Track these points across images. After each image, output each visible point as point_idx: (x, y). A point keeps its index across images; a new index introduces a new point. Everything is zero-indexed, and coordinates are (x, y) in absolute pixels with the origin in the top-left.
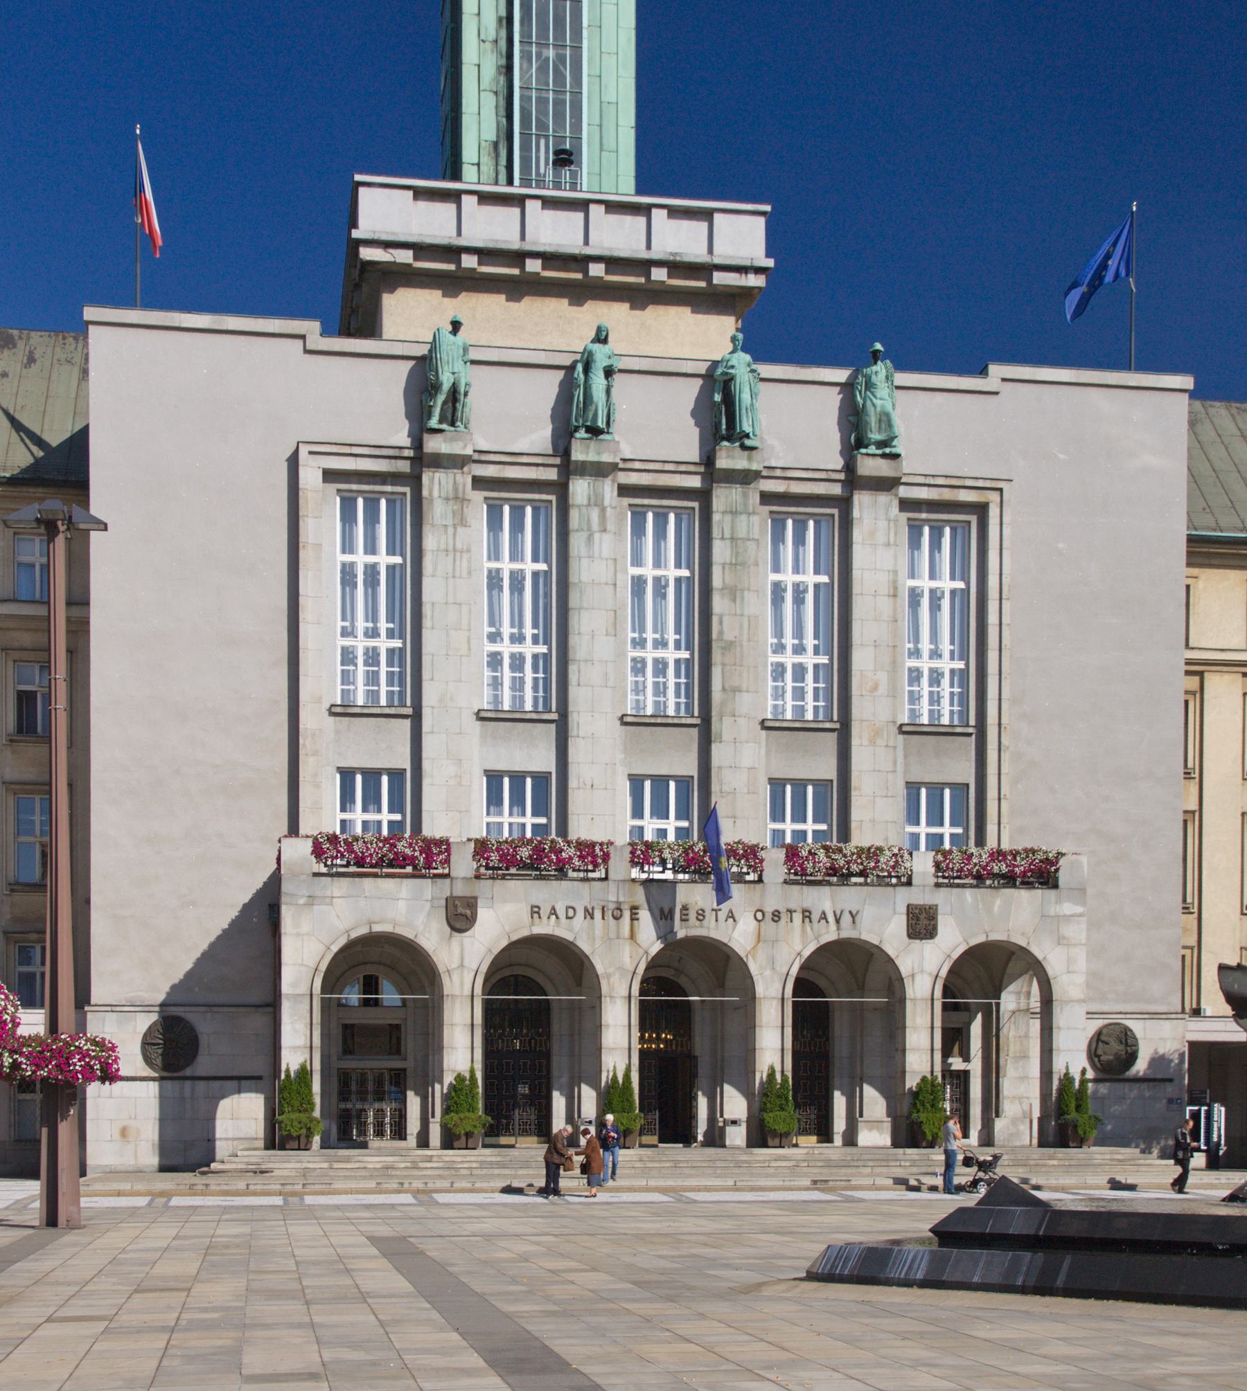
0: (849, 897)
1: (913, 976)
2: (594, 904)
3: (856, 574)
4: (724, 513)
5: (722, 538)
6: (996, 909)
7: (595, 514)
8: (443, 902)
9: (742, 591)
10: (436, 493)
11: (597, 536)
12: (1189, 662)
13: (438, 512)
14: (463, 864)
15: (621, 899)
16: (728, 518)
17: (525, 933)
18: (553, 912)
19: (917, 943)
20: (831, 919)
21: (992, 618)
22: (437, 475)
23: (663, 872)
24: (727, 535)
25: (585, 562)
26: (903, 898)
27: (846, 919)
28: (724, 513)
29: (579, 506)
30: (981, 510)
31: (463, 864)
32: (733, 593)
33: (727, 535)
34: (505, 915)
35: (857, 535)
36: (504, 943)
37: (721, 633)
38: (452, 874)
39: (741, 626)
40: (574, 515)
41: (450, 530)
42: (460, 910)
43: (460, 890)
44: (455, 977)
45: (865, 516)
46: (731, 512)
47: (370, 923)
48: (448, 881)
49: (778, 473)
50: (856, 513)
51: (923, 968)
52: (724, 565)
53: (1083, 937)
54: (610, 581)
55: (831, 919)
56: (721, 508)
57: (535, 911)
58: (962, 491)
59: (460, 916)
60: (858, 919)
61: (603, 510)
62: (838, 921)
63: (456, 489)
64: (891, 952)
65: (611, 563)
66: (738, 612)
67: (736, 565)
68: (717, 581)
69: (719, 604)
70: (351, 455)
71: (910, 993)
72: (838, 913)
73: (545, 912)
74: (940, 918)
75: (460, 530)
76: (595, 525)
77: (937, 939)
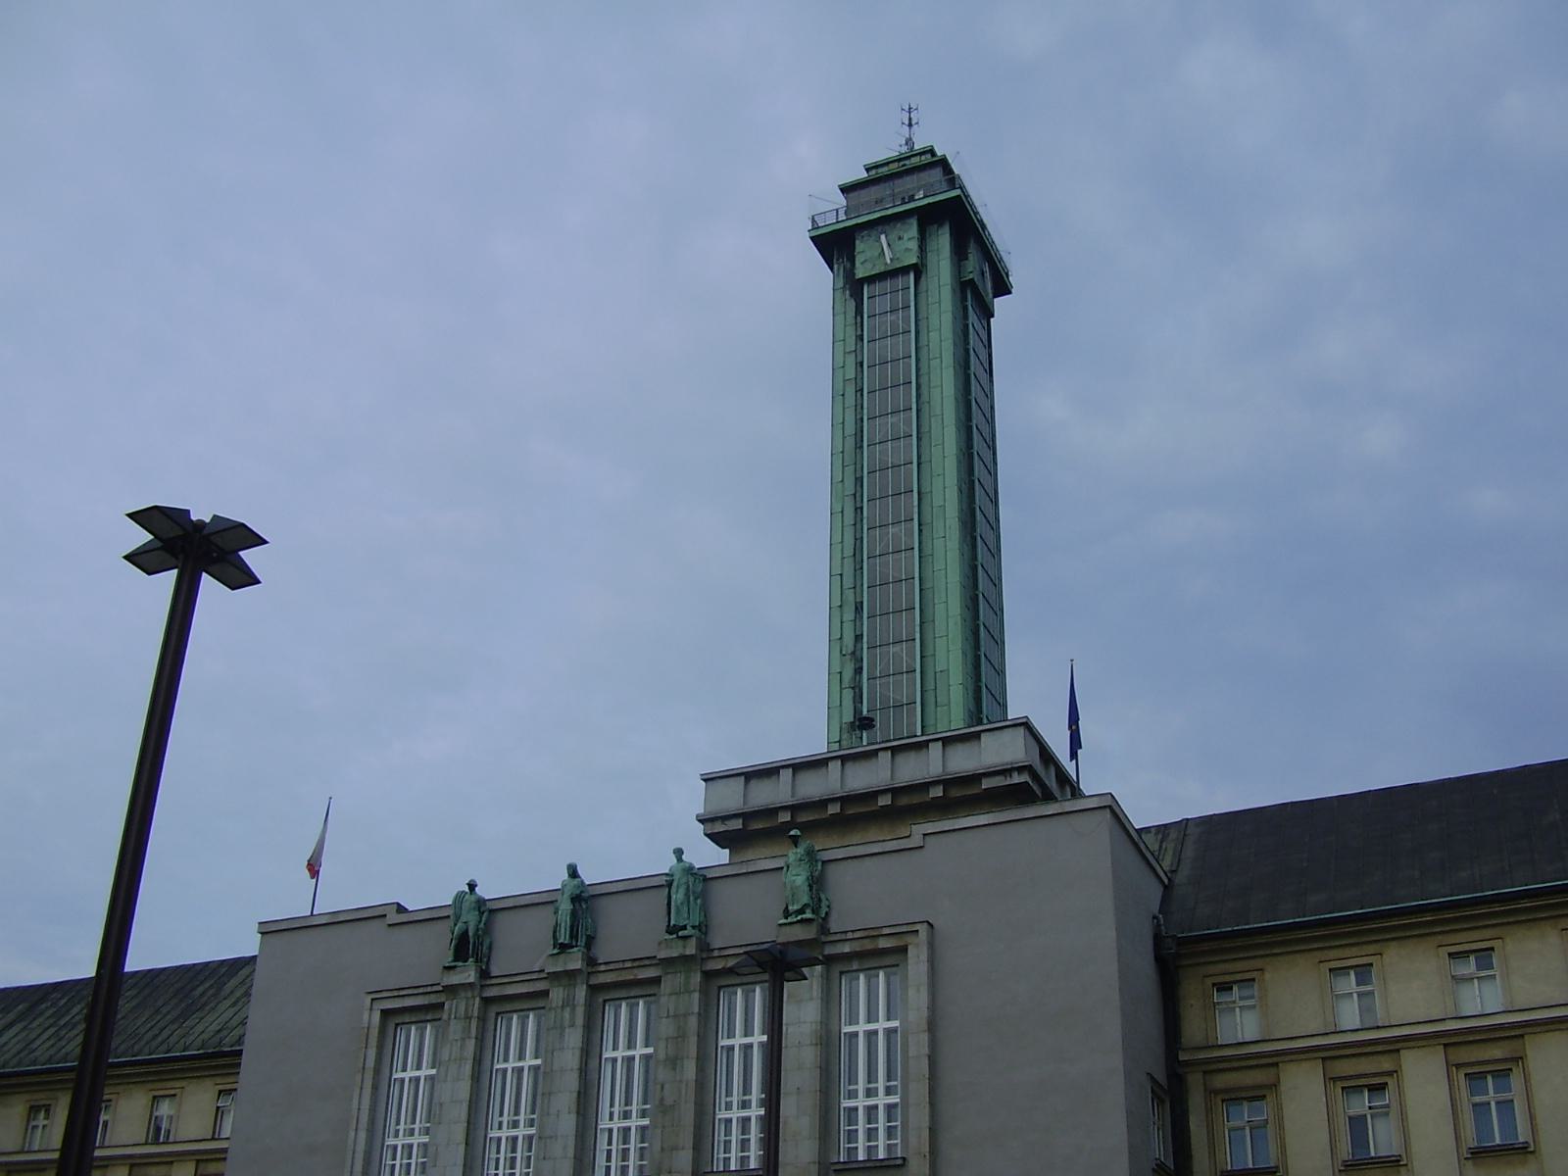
5: (668, 1017)
7: (567, 1015)
9: (682, 1059)
11: (567, 1030)
24: (671, 1013)
28: (671, 994)
30: (904, 950)
32: (674, 1062)
37: (662, 1099)
46: (676, 994)
52: (667, 1039)
56: (668, 991)
58: (881, 938)
66: (678, 1078)
75: (467, 1041)
76: (567, 1023)
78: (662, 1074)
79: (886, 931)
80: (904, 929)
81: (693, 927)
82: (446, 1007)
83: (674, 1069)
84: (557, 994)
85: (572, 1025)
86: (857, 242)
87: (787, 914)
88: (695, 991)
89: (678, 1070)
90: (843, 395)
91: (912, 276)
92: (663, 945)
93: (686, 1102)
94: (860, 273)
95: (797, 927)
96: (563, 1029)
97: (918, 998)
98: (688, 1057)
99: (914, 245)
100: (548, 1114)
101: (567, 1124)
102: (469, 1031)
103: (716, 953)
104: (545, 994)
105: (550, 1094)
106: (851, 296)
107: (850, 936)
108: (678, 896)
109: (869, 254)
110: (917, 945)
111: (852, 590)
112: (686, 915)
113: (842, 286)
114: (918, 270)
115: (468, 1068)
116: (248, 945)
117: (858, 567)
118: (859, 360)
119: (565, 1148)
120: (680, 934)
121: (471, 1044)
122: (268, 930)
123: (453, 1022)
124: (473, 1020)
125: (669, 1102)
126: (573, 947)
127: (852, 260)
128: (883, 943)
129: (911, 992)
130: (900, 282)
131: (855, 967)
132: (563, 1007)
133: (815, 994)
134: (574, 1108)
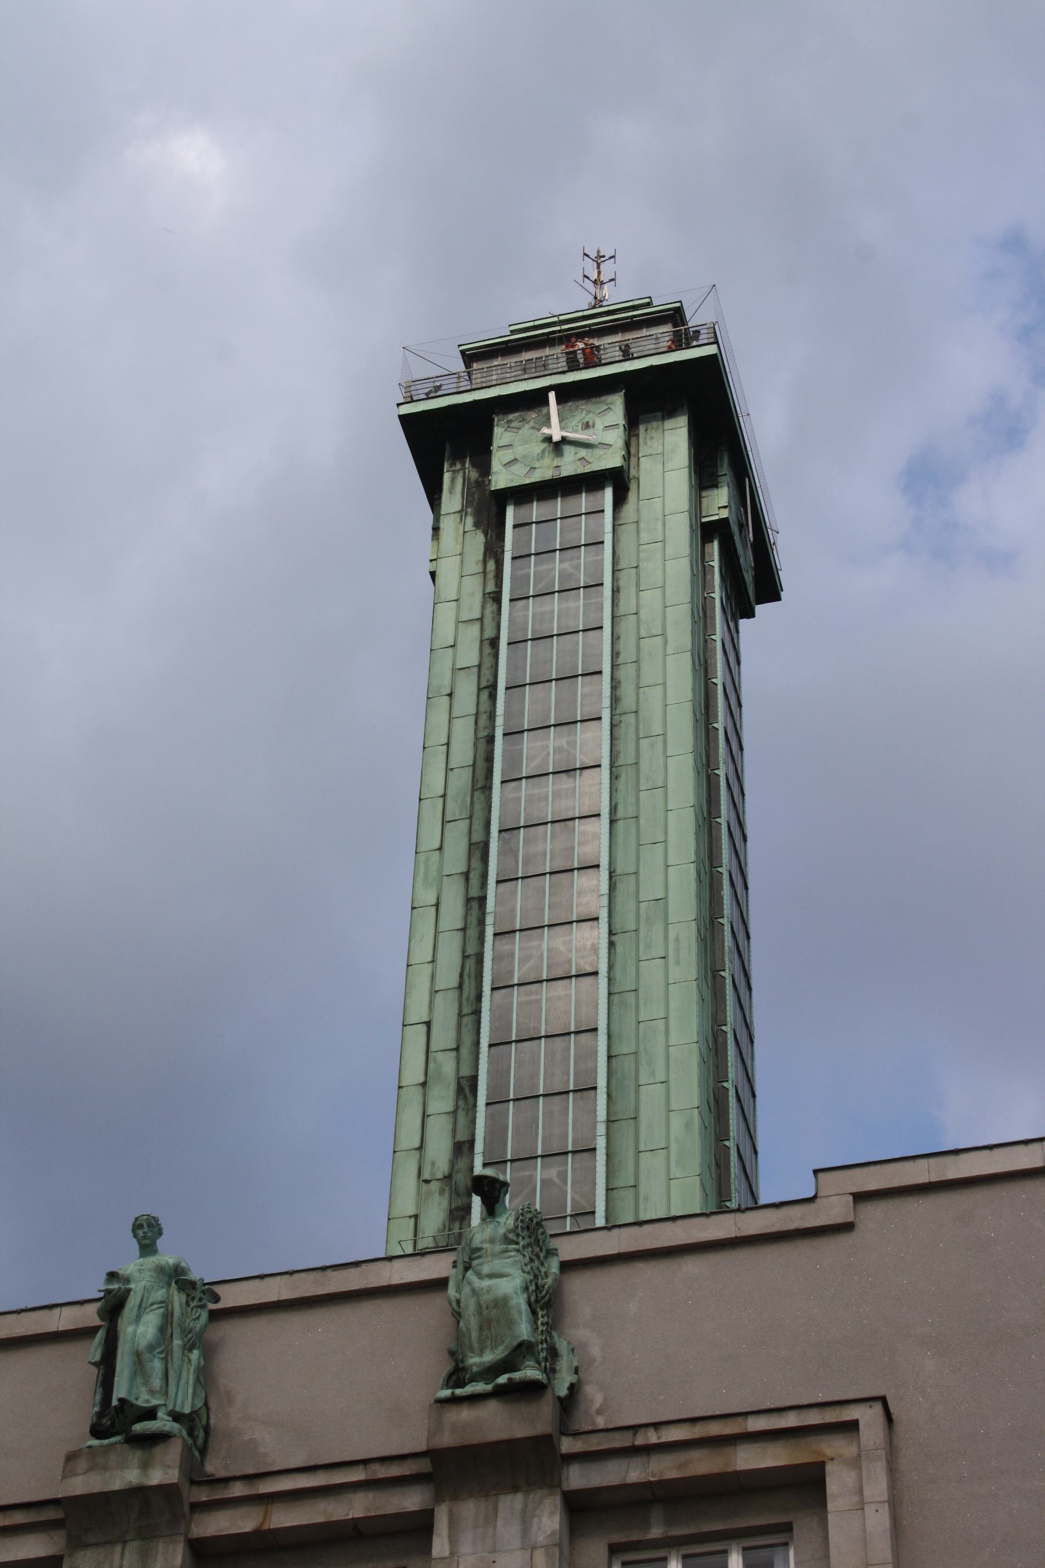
45: (466, 1547)
49: (238, 1490)
80: (813, 1418)
81: (177, 1417)
86: (497, 431)
87: (457, 1376)
90: (450, 695)
91: (609, 493)
92: (82, 1464)
94: (501, 479)
95: (492, 1406)
99: (616, 438)
106: (477, 525)
108: (140, 1330)
109: (519, 451)
110: (855, 1463)
111: (454, 1053)
112: (157, 1382)
113: (458, 508)
114: (619, 481)
117: (466, 1010)
118: (489, 633)
120: (138, 1427)
127: (485, 469)
128: (749, 1459)
130: (584, 501)
131: (656, 1532)
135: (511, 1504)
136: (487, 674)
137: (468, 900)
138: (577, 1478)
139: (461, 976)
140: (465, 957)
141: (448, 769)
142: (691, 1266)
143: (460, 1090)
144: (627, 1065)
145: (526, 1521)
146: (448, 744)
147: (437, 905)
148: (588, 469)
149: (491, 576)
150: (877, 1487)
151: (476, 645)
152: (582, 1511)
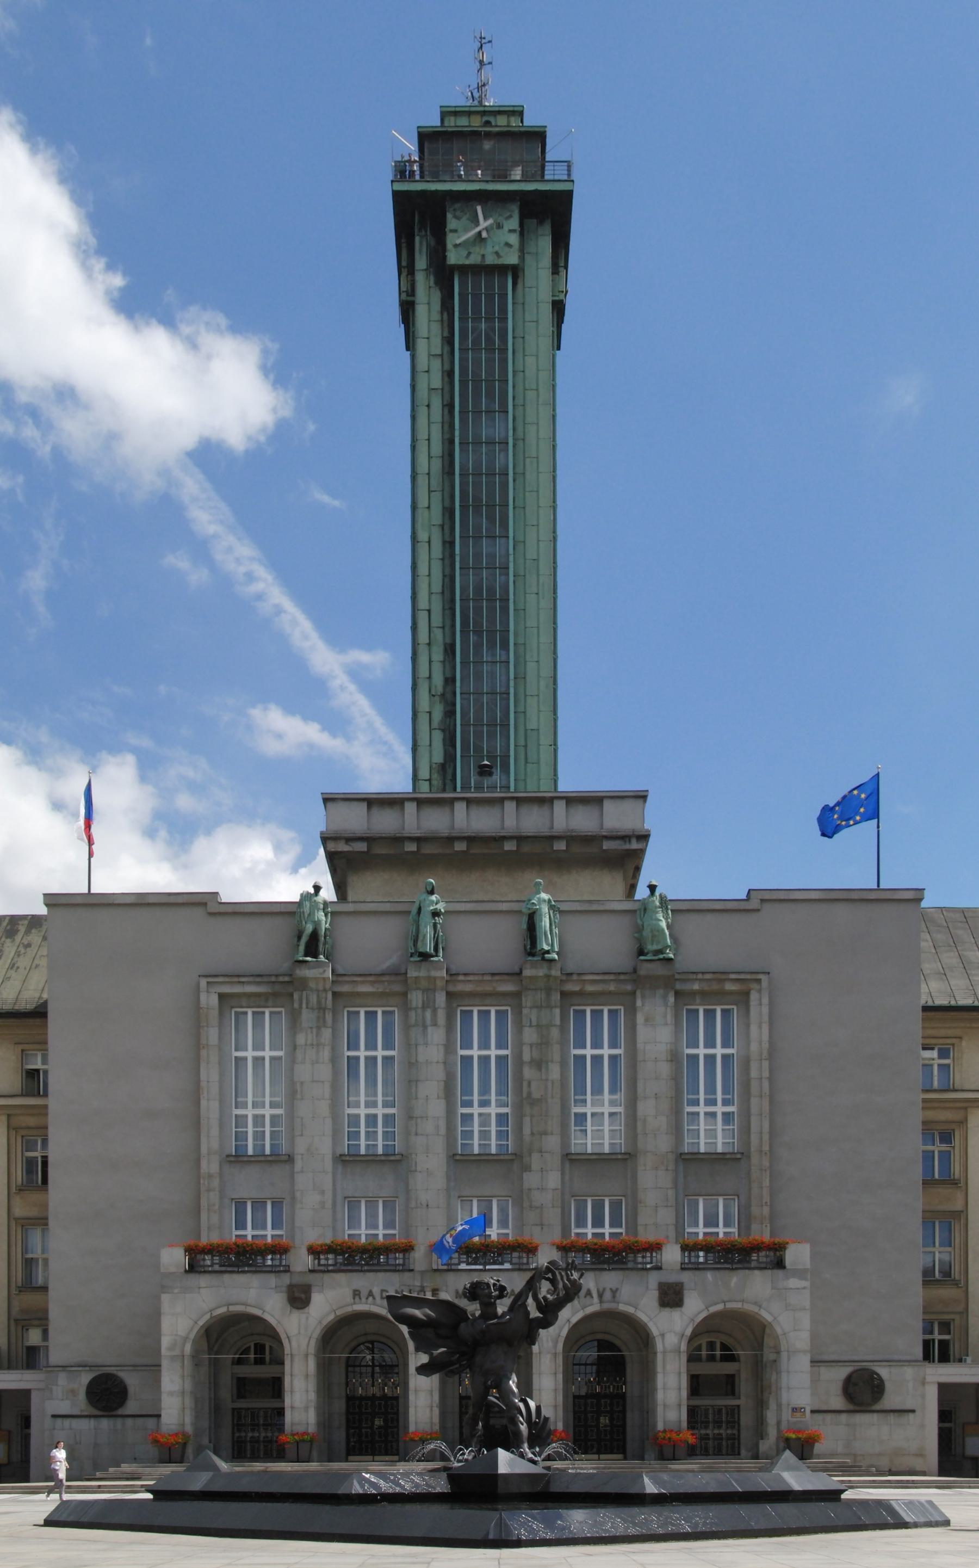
0: (610, 1279)
1: (663, 1335)
2: (403, 1288)
3: (640, 1046)
4: (531, 1008)
5: (531, 1026)
6: (732, 1284)
7: (428, 1014)
8: (284, 1289)
9: (547, 1062)
10: (304, 1006)
12: (924, 1101)
13: (307, 1017)
14: (301, 1261)
15: (425, 1284)
16: (535, 1011)
17: (349, 1309)
18: (371, 1294)
19: (666, 1312)
20: (595, 1295)
21: (754, 1074)
22: (304, 993)
23: (459, 1264)
24: (534, 1023)
25: (421, 1049)
26: (654, 1279)
27: (608, 1295)
28: (531, 1008)
29: (416, 1009)
31: (301, 1261)
32: (539, 1064)
33: (534, 1023)
34: (332, 1298)
35: (640, 1018)
36: (331, 1317)
37: (529, 1094)
38: (292, 1269)
39: (546, 1087)
40: (412, 1014)
41: (314, 1030)
42: (297, 1295)
43: (297, 1280)
44: (294, 1343)
46: (537, 1007)
47: (229, 1305)
48: (288, 1274)
50: (639, 1003)
51: (671, 1330)
52: (531, 1045)
53: (807, 1304)
54: (441, 1061)
55: (595, 1295)
56: (529, 1004)
57: (356, 1293)
59: (299, 1298)
60: (617, 1295)
61: (435, 1011)
62: (600, 1296)
63: (319, 1002)
64: (643, 1317)
65: (442, 1049)
66: (544, 1077)
67: (544, 1043)
68: (526, 1057)
69: (528, 1073)
70: (239, 982)
71: (659, 1347)
72: (601, 1290)
73: (364, 1293)
74: (685, 1292)
77: (684, 1309)
78: (528, 1073)
79: (733, 976)
82: (296, 996)
83: (540, 1069)
84: (416, 998)
85: (435, 1024)
88: (556, 1007)
89: (543, 1070)
93: (552, 1097)
96: (425, 1027)
97: (759, 1034)
98: (552, 1061)
100: (416, 1098)
101: (437, 1108)
102: (324, 1021)
103: (575, 977)
104: (405, 994)
105: (417, 1081)
106: (436, 283)
107: (700, 976)
110: (760, 991)
115: (326, 1053)
116: (43, 911)
119: (437, 1127)
121: (327, 1033)
122: (52, 900)
123: (304, 1011)
124: (327, 1012)
125: (536, 1095)
126: (433, 956)
128: (729, 987)
129: (754, 1028)
132: (424, 1008)
133: (669, 1022)
134: (442, 1094)
135: (660, 992)
136: (447, 397)
137: (444, 542)
138: (678, 986)
139: (443, 586)
140: (444, 576)
141: (430, 457)
142: (709, 917)
143: (445, 650)
144: (521, 649)
145: (665, 997)
146: (429, 440)
147: (429, 542)
148: (500, 262)
149: (446, 324)
150: (765, 1000)
151: (440, 374)
152: (678, 994)
